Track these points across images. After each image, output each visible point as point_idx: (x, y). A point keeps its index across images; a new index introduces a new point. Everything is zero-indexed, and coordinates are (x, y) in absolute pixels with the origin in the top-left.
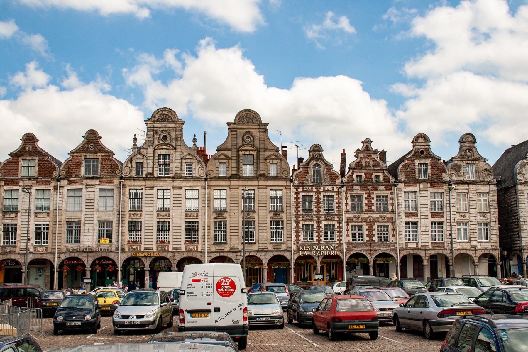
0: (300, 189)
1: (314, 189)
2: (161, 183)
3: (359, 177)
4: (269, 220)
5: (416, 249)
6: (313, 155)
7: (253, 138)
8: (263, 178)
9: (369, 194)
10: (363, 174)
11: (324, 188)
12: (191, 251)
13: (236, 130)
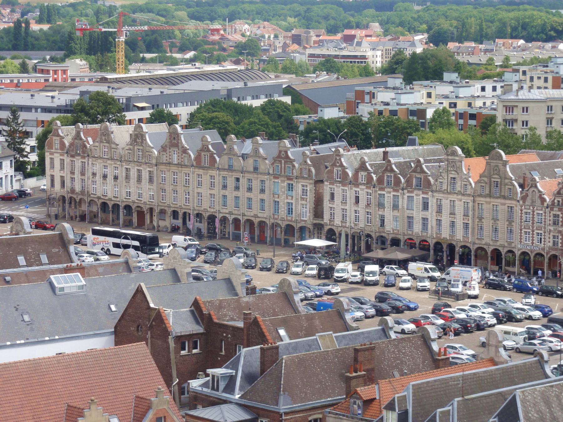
0: (523, 208)
1: (531, 208)
2: (452, 196)
3: (559, 201)
4: (506, 226)
10: (560, 200)
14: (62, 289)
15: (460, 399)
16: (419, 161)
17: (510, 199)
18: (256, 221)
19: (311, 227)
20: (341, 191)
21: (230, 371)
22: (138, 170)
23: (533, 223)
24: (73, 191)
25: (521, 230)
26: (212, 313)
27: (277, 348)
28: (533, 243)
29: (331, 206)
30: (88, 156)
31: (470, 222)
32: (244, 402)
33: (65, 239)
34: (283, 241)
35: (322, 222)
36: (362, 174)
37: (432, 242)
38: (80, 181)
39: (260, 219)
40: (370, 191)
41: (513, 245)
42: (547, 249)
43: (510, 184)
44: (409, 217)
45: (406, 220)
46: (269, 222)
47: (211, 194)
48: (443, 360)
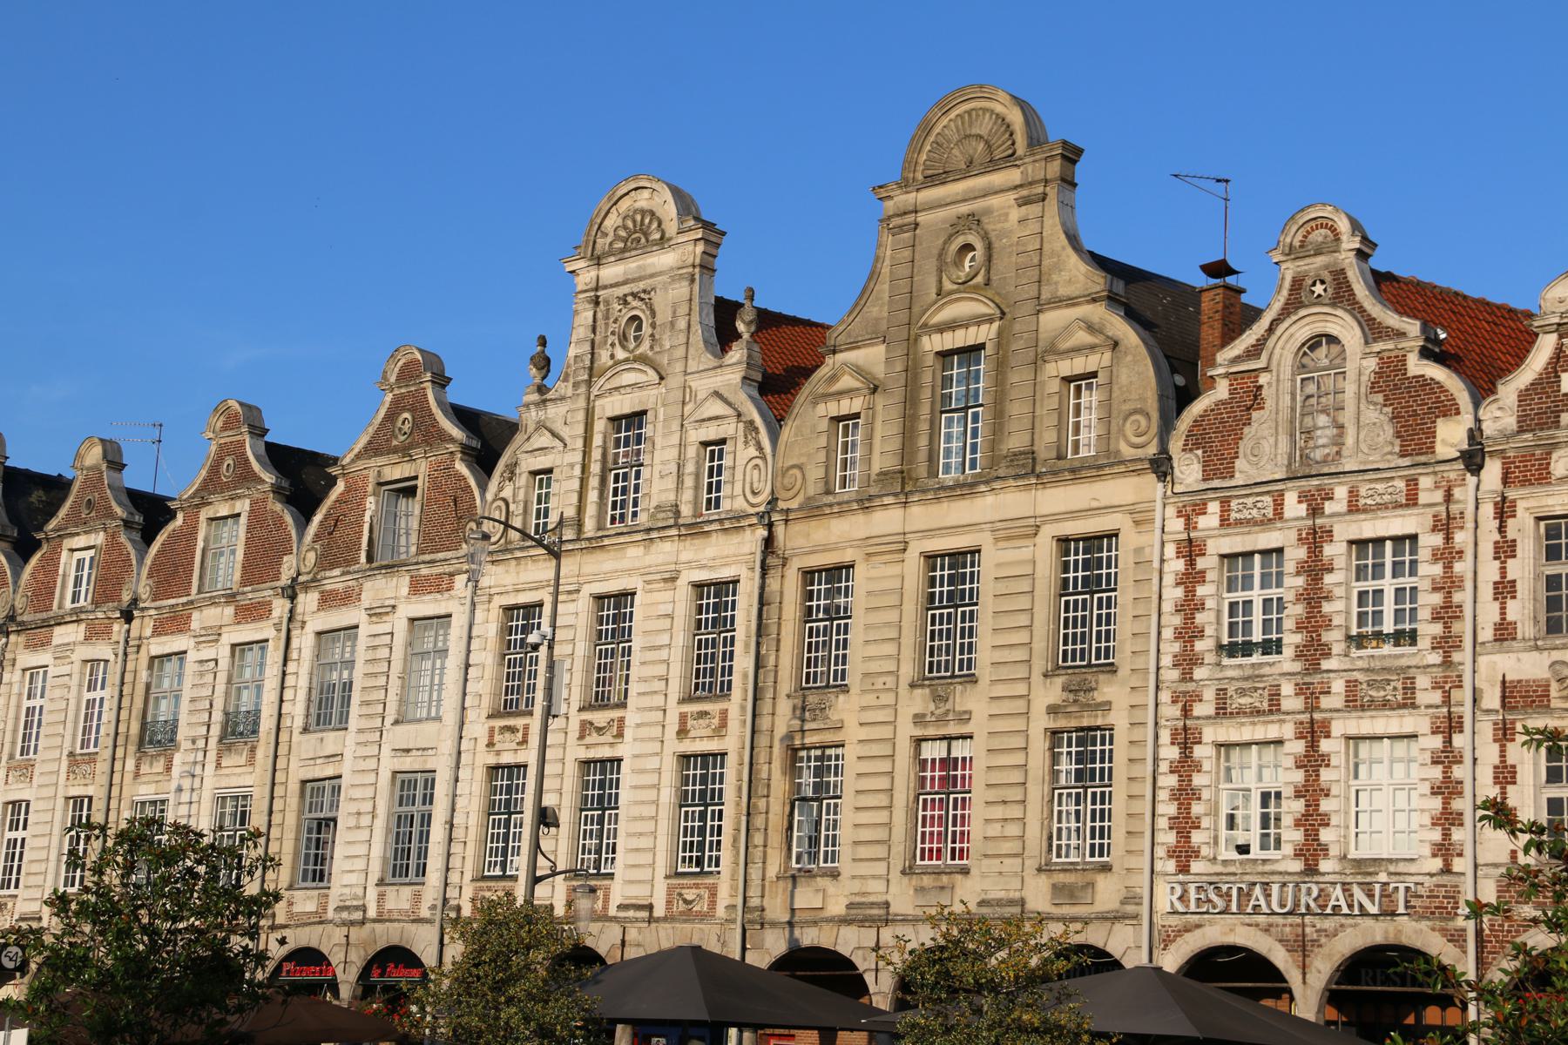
0: (1209, 520)
1: (1294, 508)
4: (1040, 723)
6: (1297, 284)
7: (989, 247)
8: (1017, 477)
11: (1354, 494)
13: (910, 218)
17: (1079, 472)
23: (1313, 653)
25: (1186, 739)
31: (733, 742)
40: (103, 650)
43: (1083, 337)
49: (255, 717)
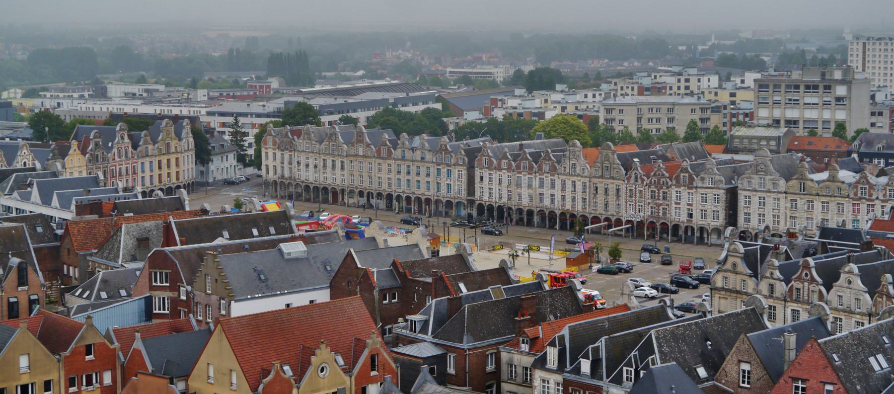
3: (655, 181)
5: (679, 222)
9: (659, 191)
10: (656, 179)
12: (584, 212)
14: (289, 254)
15: (607, 337)
16: (547, 151)
17: (617, 179)
18: (423, 198)
19: (465, 202)
20: (488, 175)
21: (425, 317)
22: (333, 160)
23: (635, 198)
24: (283, 176)
25: (626, 203)
26: (406, 271)
27: (461, 298)
28: (635, 213)
29: (481, 186)
30: (294, 150)
31: (587, 197)
32: (435, 340)
33: (288, 215)
34: (444, 213)
35: (474, 198)
36: (504, 161)
37: (558, 213)
38: (288, 169)
39: (426, 197)
40: (510, 174)
41: (620, 214)
42: (646, 217)
44: (540, 194)
45: (538, 196)
46: (433, 199)
47: (389, 178)
48: (588, 305)
49: (531, 186)
